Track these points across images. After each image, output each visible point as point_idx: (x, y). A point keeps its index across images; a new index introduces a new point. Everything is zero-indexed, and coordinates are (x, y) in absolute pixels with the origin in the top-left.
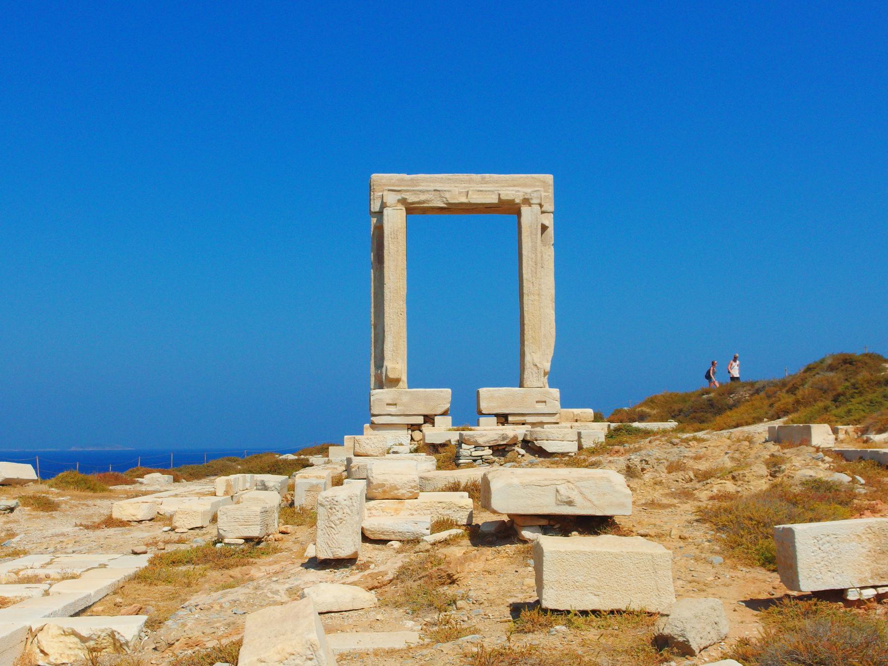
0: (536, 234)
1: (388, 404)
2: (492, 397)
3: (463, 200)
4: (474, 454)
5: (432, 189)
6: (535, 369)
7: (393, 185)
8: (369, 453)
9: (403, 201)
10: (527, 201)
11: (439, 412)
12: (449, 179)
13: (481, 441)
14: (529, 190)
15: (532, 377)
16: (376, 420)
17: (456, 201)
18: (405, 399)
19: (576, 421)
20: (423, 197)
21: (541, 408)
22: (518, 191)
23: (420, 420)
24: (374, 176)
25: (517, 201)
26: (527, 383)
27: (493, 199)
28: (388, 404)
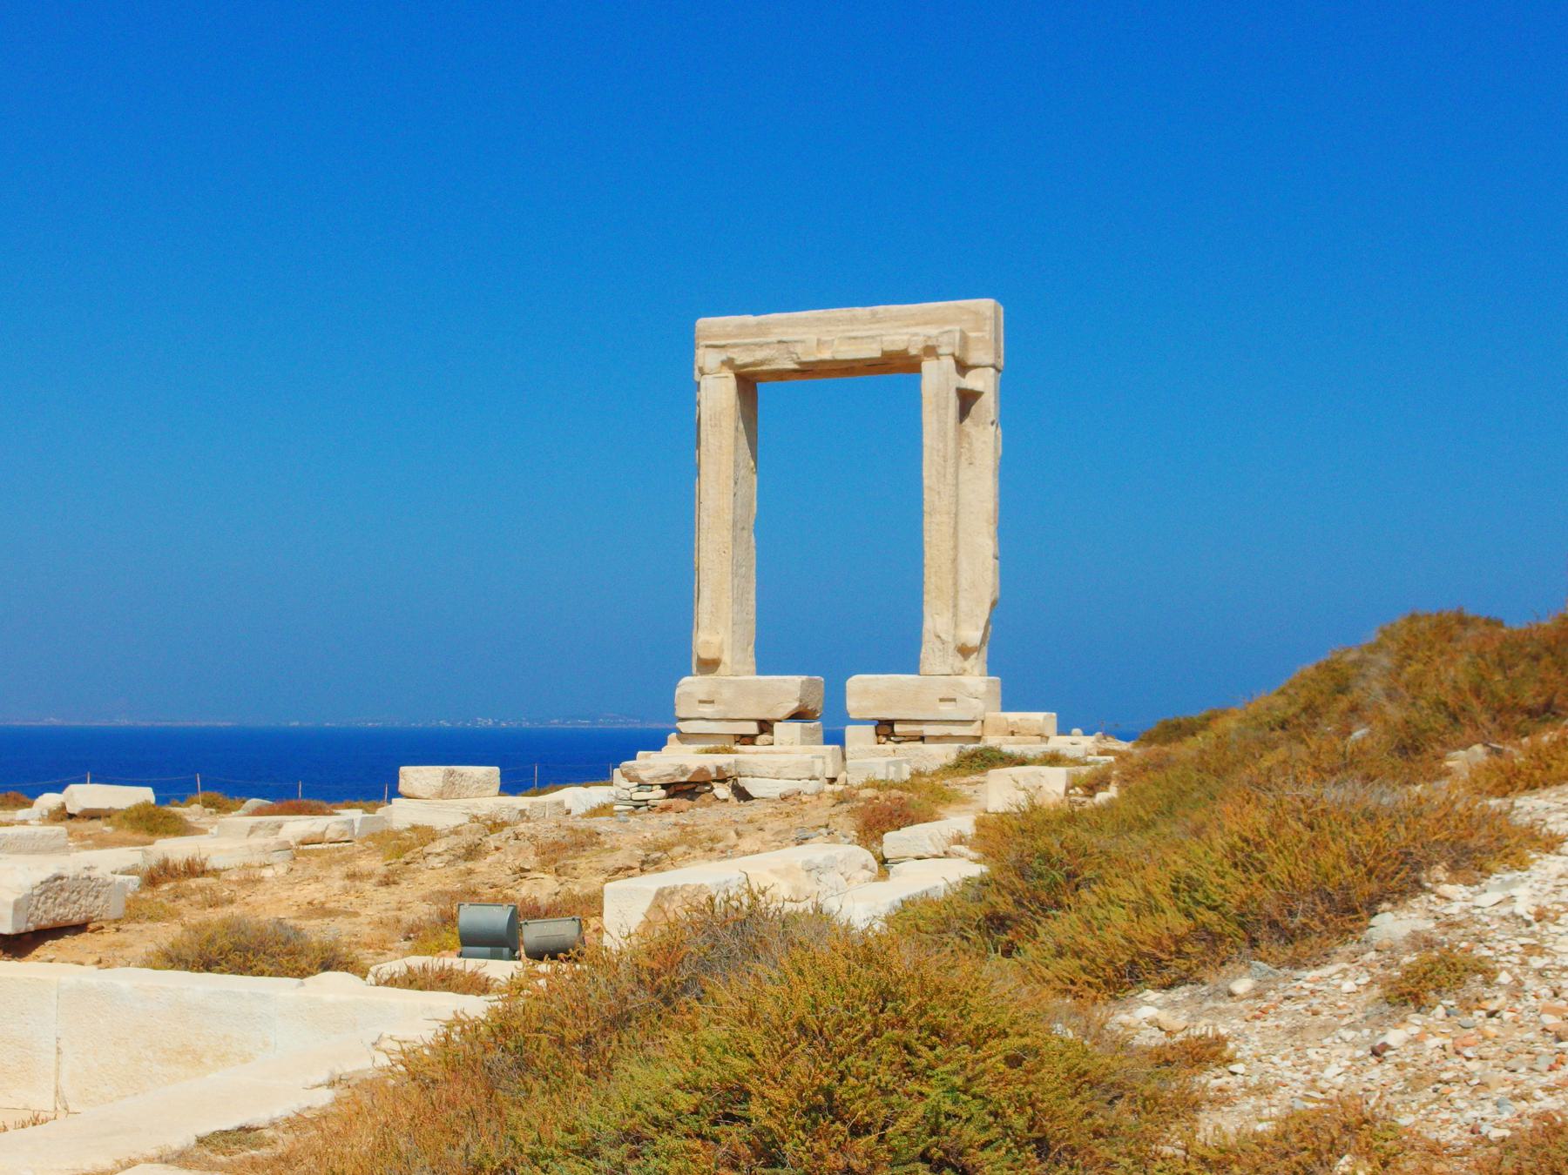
0: (946, 408)
1: (701, 702)
2: (868, 692)
3: (826, 355)
4: (635, 797)
5: (774, 339)
6: (938, 644)
7: (729, 336)
8: (418, 794)
9: (729, 363)
10: (931, 351)
11: (779, 716)
12: (818, 320)
13: (645, 776)
14: (932, 331)
15: (933, 657)
16: (680, 725)
17: (812, 358)
18: (727, 693)
19: (1013, 733)
20: (759, 355)
21: (947, 711)
22: (916, 334)
23: (752, 728)
24: (703, 323)
25: (913, 352)
26: (925, 666)
27: (871, 351)
28: (701, 702)
